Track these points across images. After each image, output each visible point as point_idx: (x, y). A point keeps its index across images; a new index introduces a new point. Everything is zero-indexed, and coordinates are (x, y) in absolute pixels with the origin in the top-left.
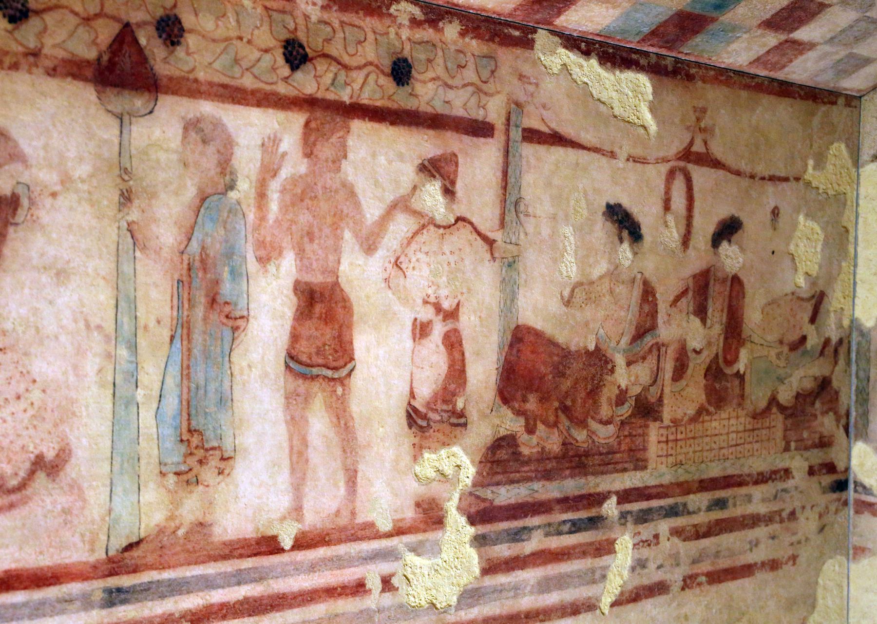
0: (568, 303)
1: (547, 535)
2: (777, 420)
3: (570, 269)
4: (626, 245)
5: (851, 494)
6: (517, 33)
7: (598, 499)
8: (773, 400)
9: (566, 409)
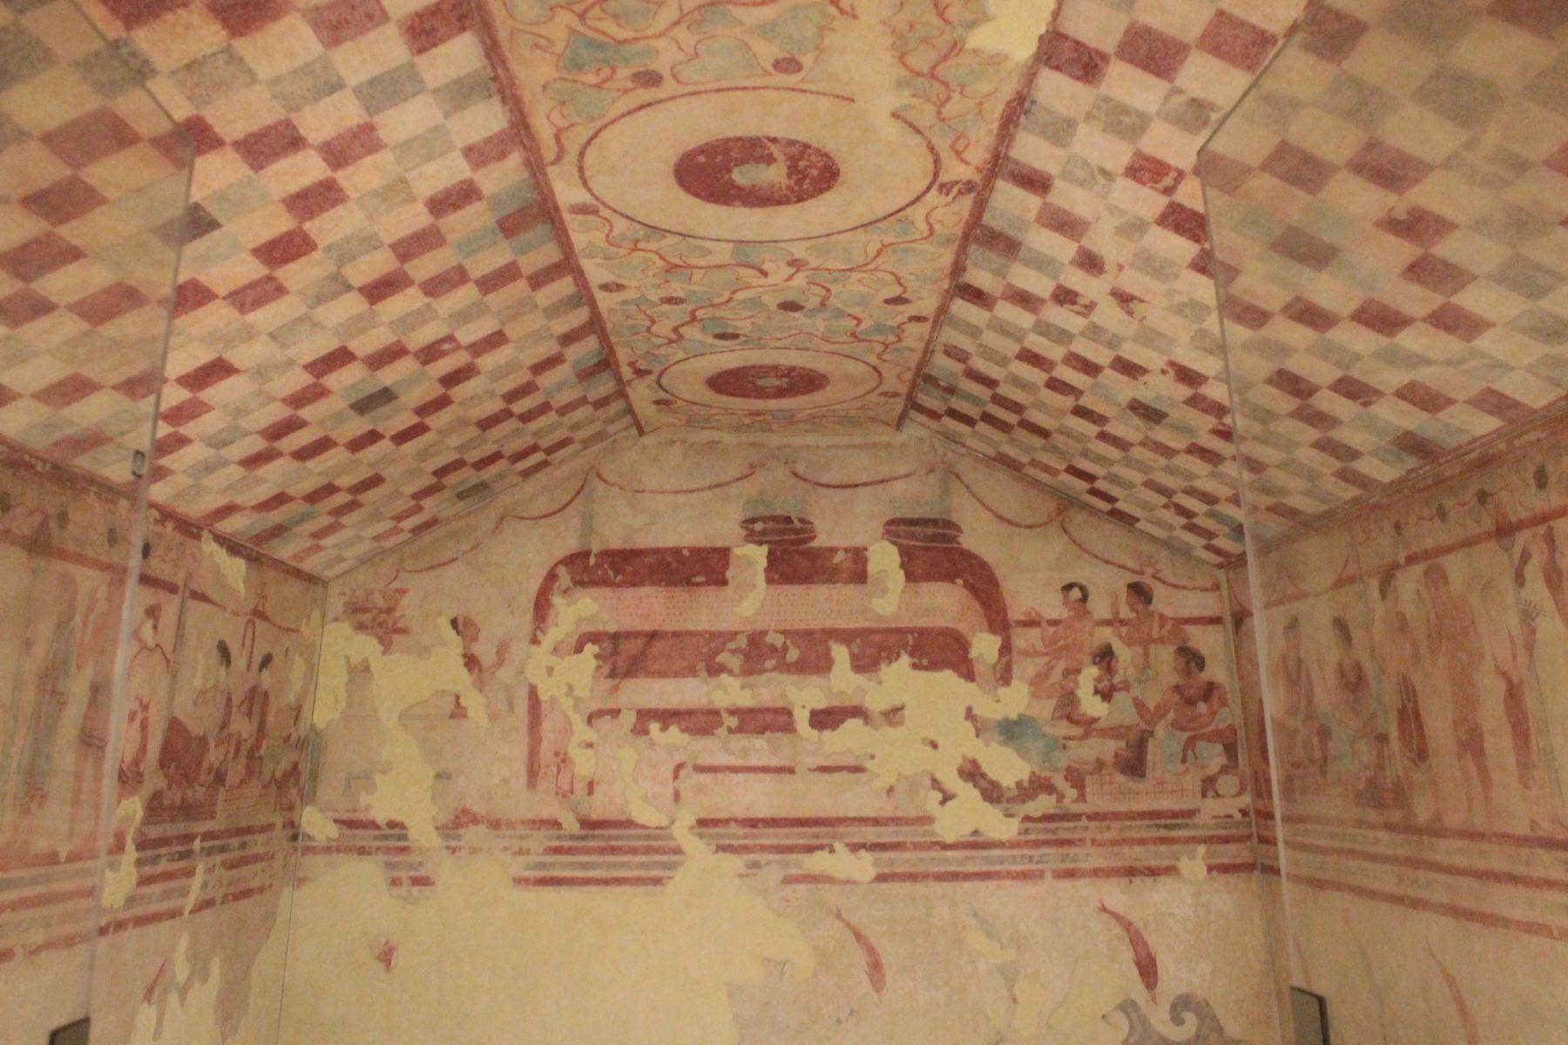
0: (195, 703)
1: (168, 860)
3: (198, 682)
4: (224, 667)
5: (300, 843)
6: (195, 531)
7: (190, 838)
8: (273, 777)
9: (186, 776)
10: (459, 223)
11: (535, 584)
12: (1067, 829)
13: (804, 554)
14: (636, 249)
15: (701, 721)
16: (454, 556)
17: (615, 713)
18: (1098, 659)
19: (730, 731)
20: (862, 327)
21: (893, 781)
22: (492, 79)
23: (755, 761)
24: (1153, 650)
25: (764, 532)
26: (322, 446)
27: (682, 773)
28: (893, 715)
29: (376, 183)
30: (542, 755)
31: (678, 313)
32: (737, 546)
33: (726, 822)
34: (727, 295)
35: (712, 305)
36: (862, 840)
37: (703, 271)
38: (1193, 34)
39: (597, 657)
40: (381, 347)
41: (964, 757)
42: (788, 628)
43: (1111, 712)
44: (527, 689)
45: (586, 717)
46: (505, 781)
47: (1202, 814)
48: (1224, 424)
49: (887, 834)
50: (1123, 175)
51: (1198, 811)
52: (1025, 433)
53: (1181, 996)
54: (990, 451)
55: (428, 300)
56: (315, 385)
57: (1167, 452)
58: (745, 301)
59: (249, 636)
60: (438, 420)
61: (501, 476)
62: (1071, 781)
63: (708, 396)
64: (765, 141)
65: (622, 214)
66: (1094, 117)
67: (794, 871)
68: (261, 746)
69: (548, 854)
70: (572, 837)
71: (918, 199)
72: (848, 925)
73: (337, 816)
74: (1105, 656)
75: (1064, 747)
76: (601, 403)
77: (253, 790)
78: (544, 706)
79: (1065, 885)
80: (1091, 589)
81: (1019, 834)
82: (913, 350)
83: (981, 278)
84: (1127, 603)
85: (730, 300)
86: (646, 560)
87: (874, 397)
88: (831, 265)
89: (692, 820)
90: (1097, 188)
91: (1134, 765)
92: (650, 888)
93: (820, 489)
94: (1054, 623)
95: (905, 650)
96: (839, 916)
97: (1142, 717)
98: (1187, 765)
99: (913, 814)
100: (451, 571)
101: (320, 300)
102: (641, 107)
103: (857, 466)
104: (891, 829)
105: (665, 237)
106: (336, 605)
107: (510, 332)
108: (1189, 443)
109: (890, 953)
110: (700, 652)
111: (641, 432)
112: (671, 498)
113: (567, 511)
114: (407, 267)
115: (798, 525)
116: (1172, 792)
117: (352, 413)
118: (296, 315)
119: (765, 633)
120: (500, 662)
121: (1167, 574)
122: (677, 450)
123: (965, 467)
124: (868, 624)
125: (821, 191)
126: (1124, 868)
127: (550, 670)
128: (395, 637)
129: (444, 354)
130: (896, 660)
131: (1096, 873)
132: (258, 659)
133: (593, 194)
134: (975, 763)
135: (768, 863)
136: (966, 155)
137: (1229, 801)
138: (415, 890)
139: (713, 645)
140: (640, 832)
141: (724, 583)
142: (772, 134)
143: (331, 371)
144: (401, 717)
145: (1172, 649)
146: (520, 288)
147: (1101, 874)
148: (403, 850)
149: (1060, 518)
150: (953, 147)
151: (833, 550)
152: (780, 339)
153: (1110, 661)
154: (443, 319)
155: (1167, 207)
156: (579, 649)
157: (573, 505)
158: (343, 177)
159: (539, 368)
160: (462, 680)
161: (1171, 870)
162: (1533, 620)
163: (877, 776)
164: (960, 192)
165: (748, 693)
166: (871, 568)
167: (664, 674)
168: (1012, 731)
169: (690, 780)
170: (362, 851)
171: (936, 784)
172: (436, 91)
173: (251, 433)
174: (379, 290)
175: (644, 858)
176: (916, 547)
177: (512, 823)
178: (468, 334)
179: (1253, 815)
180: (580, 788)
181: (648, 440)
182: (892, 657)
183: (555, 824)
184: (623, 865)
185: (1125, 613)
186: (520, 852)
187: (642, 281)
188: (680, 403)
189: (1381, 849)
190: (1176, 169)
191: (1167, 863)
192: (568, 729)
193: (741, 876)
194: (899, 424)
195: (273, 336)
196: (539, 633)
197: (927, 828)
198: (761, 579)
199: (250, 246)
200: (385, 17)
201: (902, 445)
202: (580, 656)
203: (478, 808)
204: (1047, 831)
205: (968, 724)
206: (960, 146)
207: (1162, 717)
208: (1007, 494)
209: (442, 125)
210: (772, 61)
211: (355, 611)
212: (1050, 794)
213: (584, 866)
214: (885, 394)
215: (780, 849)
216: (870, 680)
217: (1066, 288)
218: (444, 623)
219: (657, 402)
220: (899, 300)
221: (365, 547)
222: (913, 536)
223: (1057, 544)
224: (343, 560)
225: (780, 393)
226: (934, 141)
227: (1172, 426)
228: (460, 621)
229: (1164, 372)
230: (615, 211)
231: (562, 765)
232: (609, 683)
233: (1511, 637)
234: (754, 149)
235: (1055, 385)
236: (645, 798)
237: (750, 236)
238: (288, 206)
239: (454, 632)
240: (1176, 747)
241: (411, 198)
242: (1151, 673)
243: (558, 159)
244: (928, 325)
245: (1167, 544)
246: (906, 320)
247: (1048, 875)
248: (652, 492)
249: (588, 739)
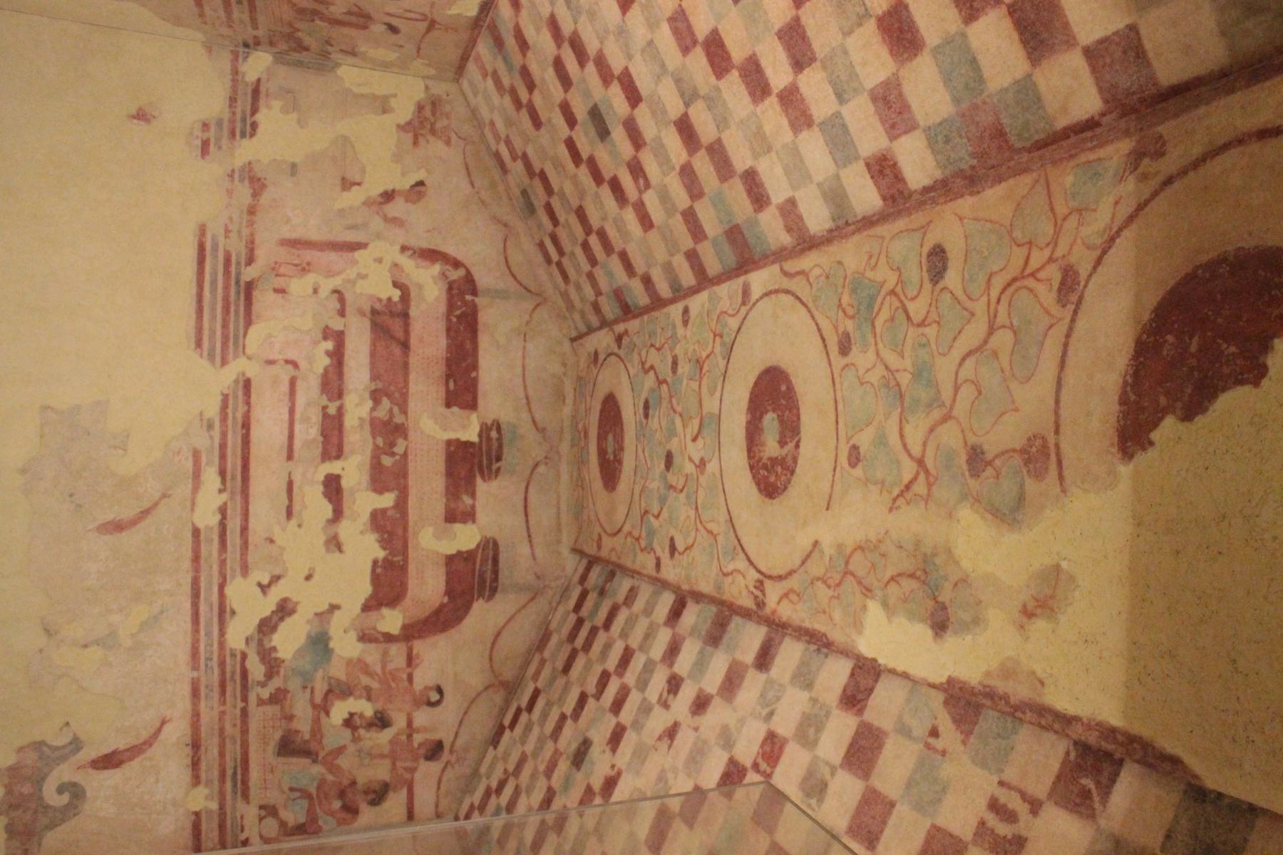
2: (287, 30)
5: (241, 49)
10: (737, 194)
11: (450, 249)
12: (234, 689)
13: (471, 470)
14: (715, 335)
15: (333, 384)
16: (476, 185)
17: (342, 313)
18: (379, 715)
19: (324, 408)
20: (652, 519)
21: (279, 542)
22: (847, 222)
23: (297, 427)
24: (387, 763)
25: (489, 439)
26: (566, 81)
27: (290, 367)
28: (335, 544)
29: (767, 129)
30: (308, 251)
31: (665, 370)
32: (478, 416)
33: (248, 403)
34: (679, 409)
35: (671, 397)
36: (228, 517)
37: (697, 390)
38: (877, 782)
39: (389, 299)
40: (641, 129)
41: (297, 603)
42: (410, 457)
43: (334, 727)
44: (363, 241)
45: (339, 288)
46: (288, 221)
49: (234, 538)
50: (769, 729)
51: (248, 803)
52: (567, 654)
54: (553, 626)
55: (678, 168)
56: (612, 76)
57: (549, 772)
58: (673, 423)
59: (413, 16)
60: (584, 174)
61: (540, 226)
62: (276, 693)
63: (600, 394)
64: (797, 439)
65: (742, 323)
66: (813, 705)
67: (204, 459)
68: (323, 21)
69: (225, 255)
70: (238, 274)
71: (751, 563)
72: (156, 504)
73: (263, 81)
74: (381, 721)
75: (305, 688)
76: (596, 308)
77: (287, 13)
78: (350, 254)
79: (187, 689)
81: (231, 649)
82: (634, 562)
83: (691, 615)
84: (427, 740)
85: (675, 411)
86: (468, 342)
87: (598, 529)
88: (701, 493)
89: (249, 374)
90: (759, 708)
91: (288, 747)
92: (193, 340)
93: (524, 485)
94: (410, 678)
95: (390, 554)
96: (164, 496)
97: (331, 753)
99: (250, 559)
100: (465, 184)
101: (678, 81)
102: (823, 340)
103: (543, 516)
104: (238, 541)
105: (724, 359)
106: (439, 89)
107: (653, 236)
109: (130, 539)
110: (390, 385)
111: (573, 340)
112: (519, 363)
113: (511, 279)
114: (703, 151)
115: (495, 467)
116: (265, 780)
117: (591, 105)
118: (667, 63)
119: (406, 438)
120: (387, 219)
121: (449, 774)
122: (556, 368)
123: (541, 604)
124: (411, 524)
125: (758, 484)
126: (200, 739)
127: (379, 261)
128: (411, 135)
129: (636, 179)
130: (381, 546)
131: (196, 715)
132: (395, 22)
133: (757, 301)
134: (292, 612)
135: (211, 437)
136: (785, 601)
137: (255, 830)
138: (198, 143)
139: (397, 395)
140: (241, 332)
141: (448, 405)
142: (802, 445)
143: (623, 89)
144: (345, 139)
146: (687, 242)
147: (195, 719)
148: (233, 134)
150: (792, 591)
151: (473, 495)
152: (644, 452)
153: (377, 726)
154: (662, 180)
155: (743, 766)
156: (396, 285)
157: (515, 283)
158: (772, 103)
159: (624, 257)
160: (374, 187)
161: (196, 780)
163: (284, 530)
164: (756, 597)
165: (356, 423)
166: (458, 527)
167: (373, 355)
168: (319, 643)
169: (285, 374)
170: (233, 100)
171: (276, 579)
172: (837, 177)
173: (576, 23)
174: (685, 128)
175: (219, 333)
176: (474, 564)
177: (252, 225)
178: (650, 199)
180: (280, 282)
181: (567, 345)
182: (385, 543)
183: (250, 261)
184: (213, 317)
185: (418, 738)
186: (227, 231)
187: (691, 341)
188: (595, 371)
190: (772, 772)
191: (203, 776)
192: (330, 274)
193: (201, 414)
194: (576, 551)
195: (650, 43)
196: (410, 252)
197: (238, 570)
198: (453, 436)
199: (720, 27)
200: (893, 138)
201: (559, 553)
202: (390, 285)
203: (265, 199)
204: (233, 673)
205: (326, 607)
206: (793, 597)
207: (331, 772)
208: (518, 638)
209: (812, 182)
210: (858, 444)
211: (433, 104)
212: (265, 675)
213: (214, 282)
214: (600, 538)
215: (223, 446)
216: (365, 524)
217: (681, 684)
218: (421, 175)
219: (596, 354)
220: (673, 549)
221: (485, 113)
222: (484, 561)
223: (476, 680)
224: (475, 95)
225: (602, 452)
226: (795, 576)
228: (422, 189)
229: (613, 766)
230: (745, 318)
231: (299, 268)
232: (367, 308)
234: (791, 430)
235: (605, 678)
236: (270, 336)
237: (723, 427)
238: (751, 57)
239: (413, 182)
240: (303, 782)
241: (756, 156)
242: (367, 761)
243: (785, 274)
244: (654, 573)
245: (475, 774)
246: (658, 554)
247: (195, 674)
248: (525, 348)
249: (320, 291)
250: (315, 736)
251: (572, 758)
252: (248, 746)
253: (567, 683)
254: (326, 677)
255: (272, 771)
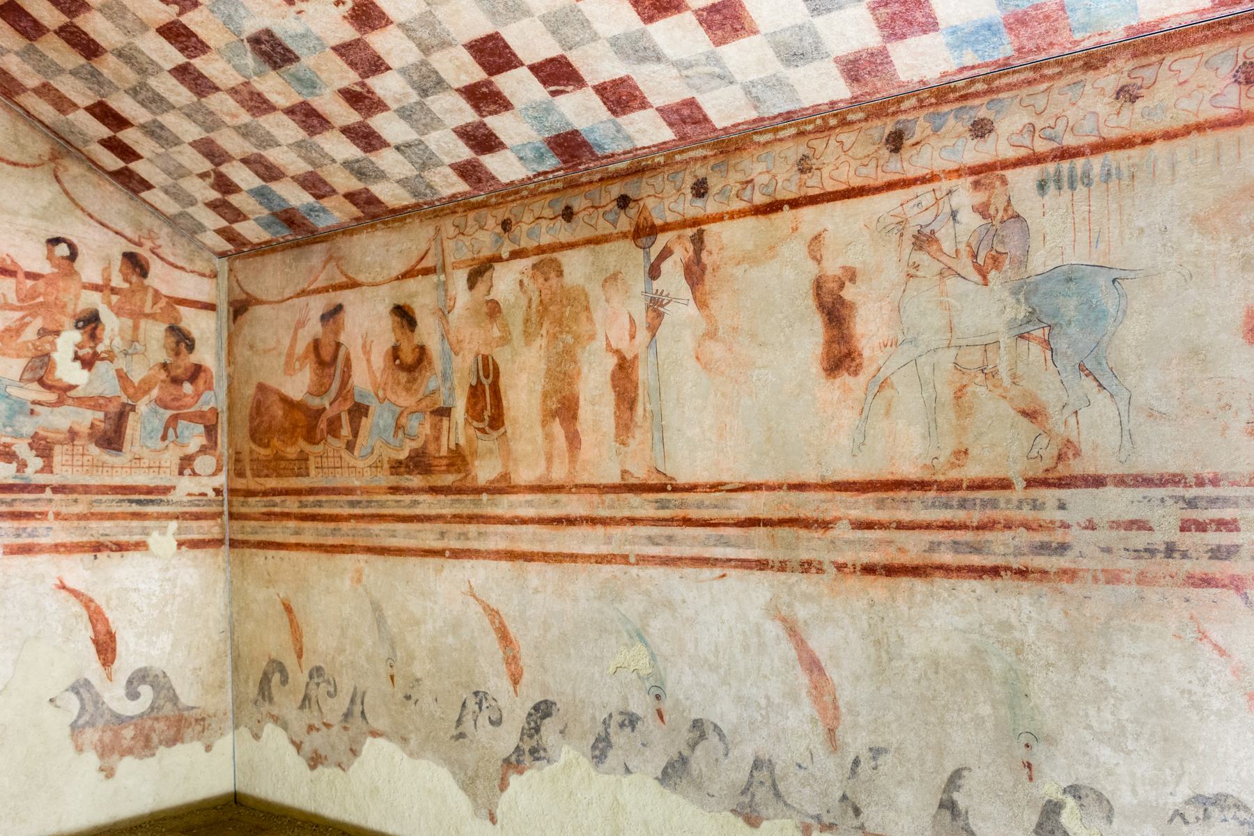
12: (25, 501)
18: (81, 324)
24: (143, 323)
43: (90, 382)
47: (177, 490)
48: (363, 85)
51: (174, 488)
53: (140, 670)
62: (36, 450)
74: (90, 322)
75: (32, 412)
79: (20, 561)
80: (81, 249)
84: (120, 271)
91: (111, 438)
97: (124, 389)
98: (167, 442)
108: (301, 99)
121: (166, 252)
126: (90, 542)
131: (56, 548)
137: (205, 480)
145: (164, 326)
147: (62, 549)
149: (53, 165)
153: (95, 328)
161: (140, 546)
162: (662, 306)
179: (225, 495)
185: (117, 281)
189: (418, 511)
223: (47, 192)
227: (292, 75)
233: (632, 321)
240: (158, 424)
245: (171, 221)
250: (100, 406)
251: (267, 68)
252: (104, 486)
253: (120, 54)
254: (22, 384)
255: (139, 459)
